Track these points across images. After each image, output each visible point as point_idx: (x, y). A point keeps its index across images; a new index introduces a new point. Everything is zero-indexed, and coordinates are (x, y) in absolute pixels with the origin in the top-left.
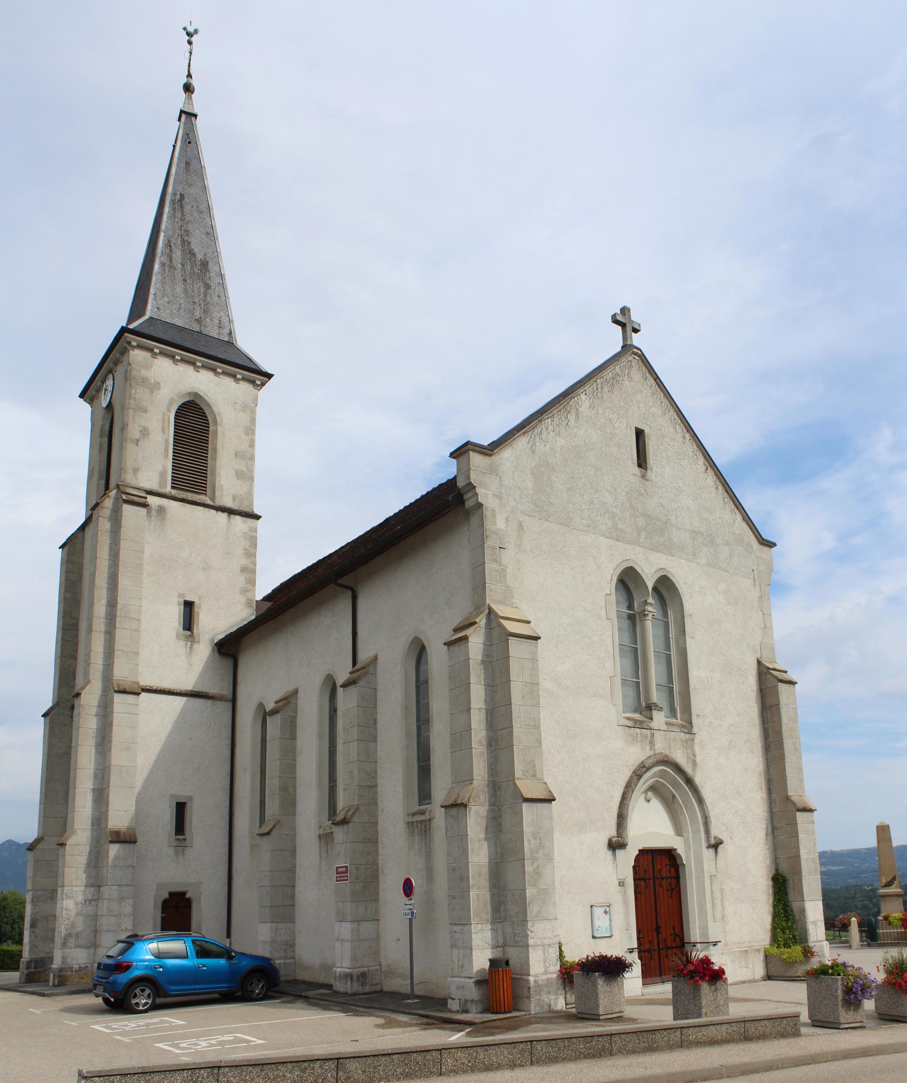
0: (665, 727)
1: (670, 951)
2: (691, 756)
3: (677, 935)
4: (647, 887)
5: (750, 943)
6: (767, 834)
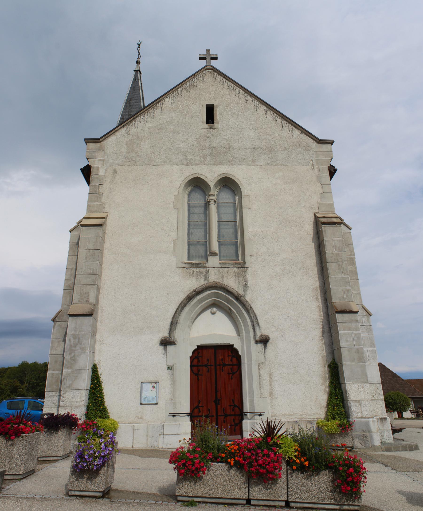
0: (220, 266)
2: (243, 282)
3: (235, 406)
4: (208, 371)
5: (301, 415)
6: (323, 332)
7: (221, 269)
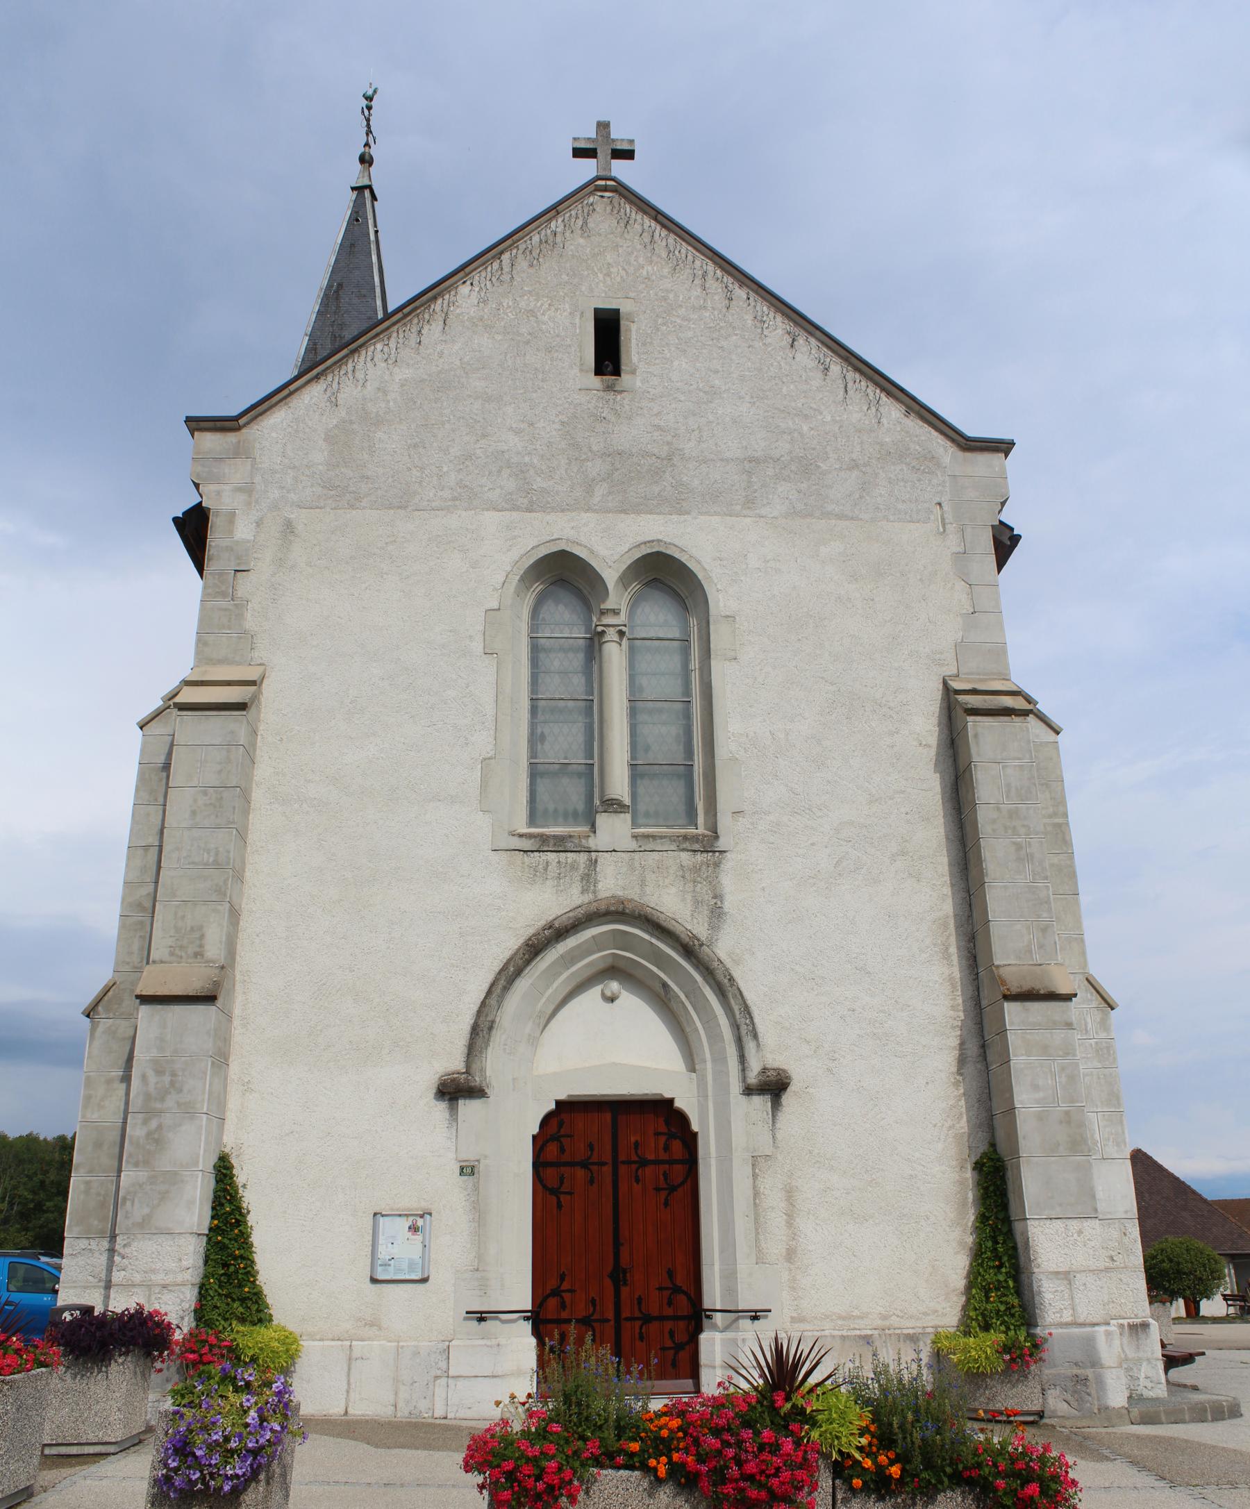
0: (633, 845)
1: (654, 1326)
3: (677, 1290)
4: (592, 1182)
5: (885, 1318)
6: (962, 1061)
7: (637, 855)
